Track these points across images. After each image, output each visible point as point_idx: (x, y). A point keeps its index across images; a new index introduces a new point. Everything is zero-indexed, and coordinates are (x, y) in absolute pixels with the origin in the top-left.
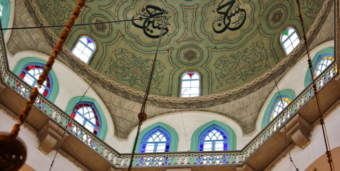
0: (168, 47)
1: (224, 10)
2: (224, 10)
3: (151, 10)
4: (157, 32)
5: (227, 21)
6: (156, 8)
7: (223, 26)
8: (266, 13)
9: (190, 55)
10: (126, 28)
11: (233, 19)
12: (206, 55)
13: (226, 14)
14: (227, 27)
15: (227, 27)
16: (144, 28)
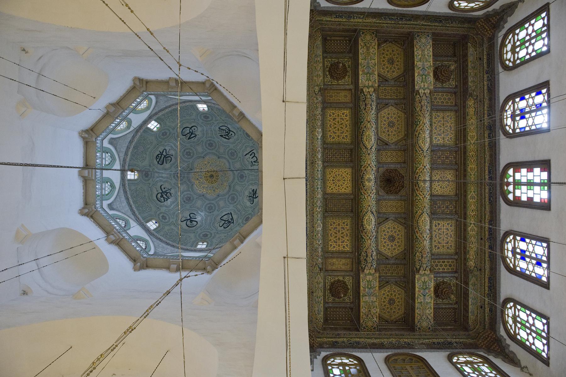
0: (218, 121)
1: (193, 135)
2: (193, 135)
3: (227, 137)
4: (224, 128)
5: (191, 131)
6: (225, 138)
7: (193, 129)
8: (171, 135)
9: (205, 117)
10: (237, 132)
11: (188, 132)
12: (199, 117)
13: (192, 134)
14: (191, 128)
15: (191, 128)
16: (230, 131)
